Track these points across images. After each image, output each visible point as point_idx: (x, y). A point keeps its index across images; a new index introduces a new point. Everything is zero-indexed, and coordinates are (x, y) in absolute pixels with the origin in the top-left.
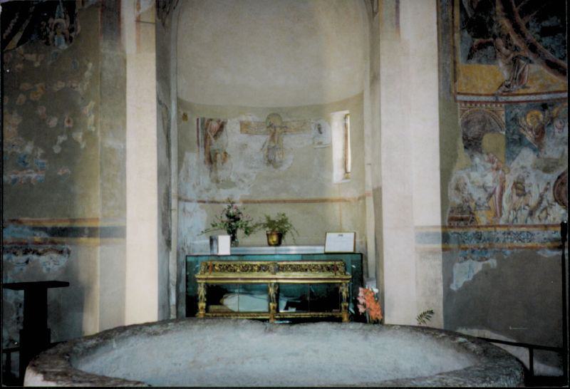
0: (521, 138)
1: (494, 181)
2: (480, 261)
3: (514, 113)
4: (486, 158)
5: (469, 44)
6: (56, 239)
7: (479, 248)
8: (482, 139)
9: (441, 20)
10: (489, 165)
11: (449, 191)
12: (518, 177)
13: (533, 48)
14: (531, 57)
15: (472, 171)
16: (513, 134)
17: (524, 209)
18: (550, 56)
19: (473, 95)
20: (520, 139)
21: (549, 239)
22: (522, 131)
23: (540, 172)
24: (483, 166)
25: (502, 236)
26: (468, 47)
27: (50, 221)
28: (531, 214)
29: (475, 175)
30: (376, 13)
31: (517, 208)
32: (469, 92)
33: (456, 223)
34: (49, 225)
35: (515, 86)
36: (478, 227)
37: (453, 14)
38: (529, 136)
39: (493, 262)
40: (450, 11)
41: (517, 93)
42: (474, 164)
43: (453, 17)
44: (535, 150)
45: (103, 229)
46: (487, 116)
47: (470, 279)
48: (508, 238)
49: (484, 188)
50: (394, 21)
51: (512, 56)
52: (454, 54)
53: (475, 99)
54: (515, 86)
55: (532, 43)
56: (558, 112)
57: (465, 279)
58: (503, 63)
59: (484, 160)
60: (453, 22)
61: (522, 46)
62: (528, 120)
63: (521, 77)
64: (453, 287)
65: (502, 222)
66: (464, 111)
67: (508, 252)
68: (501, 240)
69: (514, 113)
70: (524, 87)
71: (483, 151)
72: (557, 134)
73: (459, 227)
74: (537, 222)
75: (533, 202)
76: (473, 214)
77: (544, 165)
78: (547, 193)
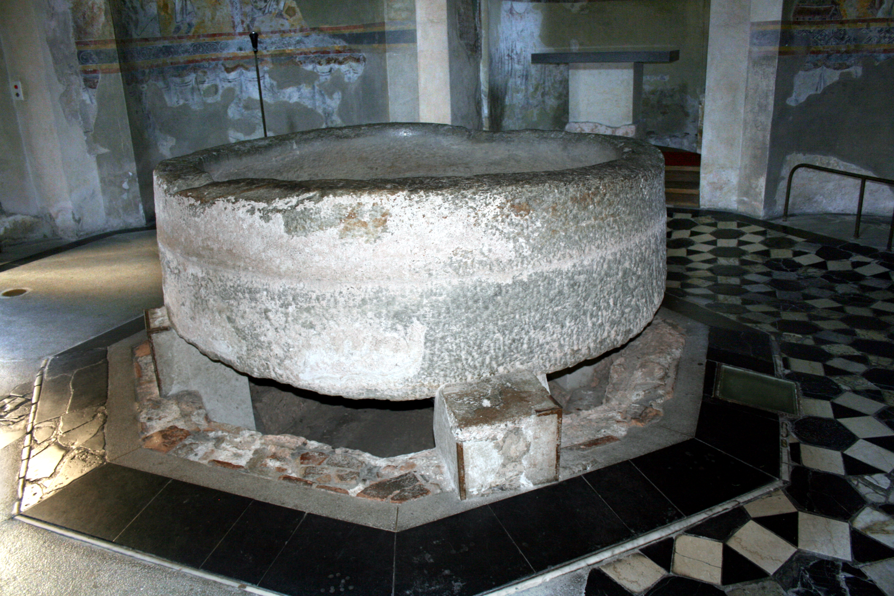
6: (354, 46)
7: (838, 52)
25: (878, 35)
27: (347, 28)
33: (807, 18)
34: (347, 32)
36: (842, 23)
39: (857, 71)
45: (392, 33)
47: (819, 92)
57: (812, 93)
67: (882, 57)
73: (811, 23)
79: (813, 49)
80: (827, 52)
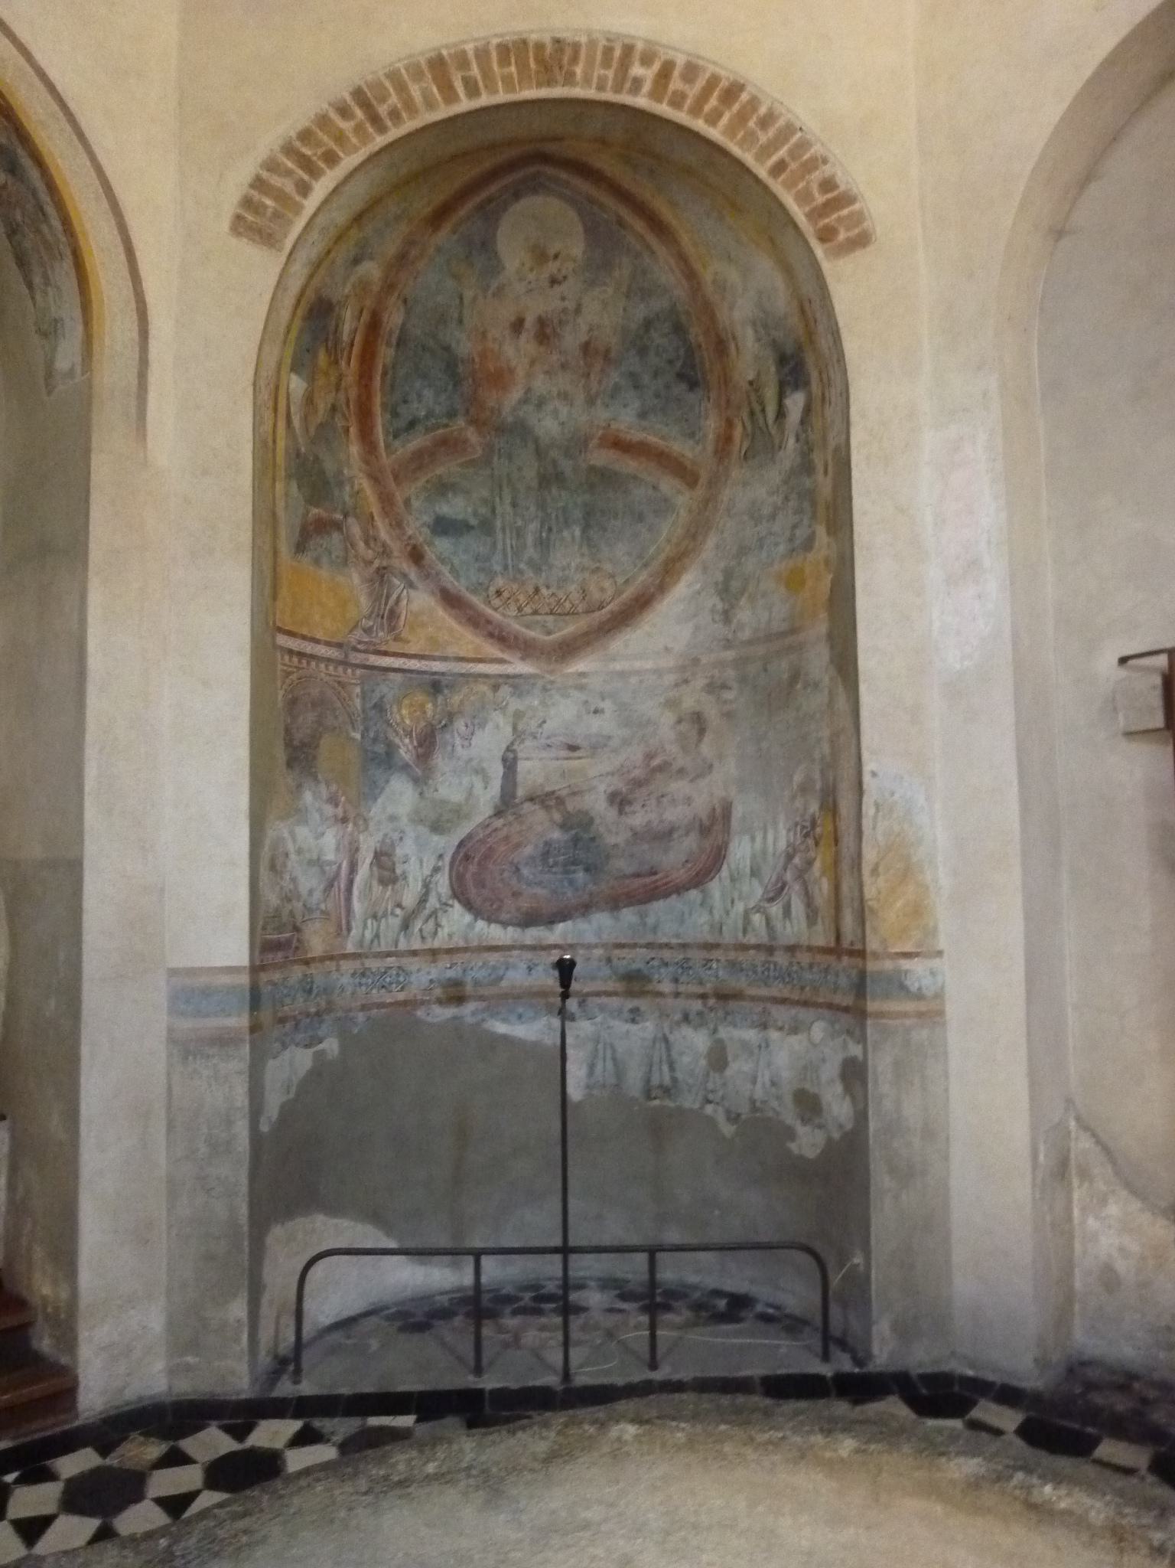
0: (391, 750)
1: (337, 849)
2: (306, 1046)
4: (323, 788)
8: (317, 747)
10: (329, 810)
12: (383, 842)
13: (416, 556)
16: (375, 740)
17: (393, 914)
18: (448, 579)
19: (304, 638)
21: (439, 981)
22: (392, 736)
23: (423, 830)
24: (320, 810)
25: (351, 980)
28: (406, 926)
29: (303, 832)
31: (380, 914)
36: (307, 962)
38: (406, 751)
39: (331, 1046)
43: (274, 441)
47: (292, 1096)
49: (318, 863)
50: (133, 411)
53: (308, 648)
56: (462, 701)
60: (274, 450)
61: (395, 546)
62: (404, 712)
64: (264, 1128)
65: (350, 948)
66: (288, 674)
67: (361, 1017)
68: (349, 990)
70: (397, 639)
71: (320, 777)
72: (459, 749)
73: (276, 966)
74: (417, 945)
75: (409, 899)
79: (280, 1014)
80: (294, 1017)
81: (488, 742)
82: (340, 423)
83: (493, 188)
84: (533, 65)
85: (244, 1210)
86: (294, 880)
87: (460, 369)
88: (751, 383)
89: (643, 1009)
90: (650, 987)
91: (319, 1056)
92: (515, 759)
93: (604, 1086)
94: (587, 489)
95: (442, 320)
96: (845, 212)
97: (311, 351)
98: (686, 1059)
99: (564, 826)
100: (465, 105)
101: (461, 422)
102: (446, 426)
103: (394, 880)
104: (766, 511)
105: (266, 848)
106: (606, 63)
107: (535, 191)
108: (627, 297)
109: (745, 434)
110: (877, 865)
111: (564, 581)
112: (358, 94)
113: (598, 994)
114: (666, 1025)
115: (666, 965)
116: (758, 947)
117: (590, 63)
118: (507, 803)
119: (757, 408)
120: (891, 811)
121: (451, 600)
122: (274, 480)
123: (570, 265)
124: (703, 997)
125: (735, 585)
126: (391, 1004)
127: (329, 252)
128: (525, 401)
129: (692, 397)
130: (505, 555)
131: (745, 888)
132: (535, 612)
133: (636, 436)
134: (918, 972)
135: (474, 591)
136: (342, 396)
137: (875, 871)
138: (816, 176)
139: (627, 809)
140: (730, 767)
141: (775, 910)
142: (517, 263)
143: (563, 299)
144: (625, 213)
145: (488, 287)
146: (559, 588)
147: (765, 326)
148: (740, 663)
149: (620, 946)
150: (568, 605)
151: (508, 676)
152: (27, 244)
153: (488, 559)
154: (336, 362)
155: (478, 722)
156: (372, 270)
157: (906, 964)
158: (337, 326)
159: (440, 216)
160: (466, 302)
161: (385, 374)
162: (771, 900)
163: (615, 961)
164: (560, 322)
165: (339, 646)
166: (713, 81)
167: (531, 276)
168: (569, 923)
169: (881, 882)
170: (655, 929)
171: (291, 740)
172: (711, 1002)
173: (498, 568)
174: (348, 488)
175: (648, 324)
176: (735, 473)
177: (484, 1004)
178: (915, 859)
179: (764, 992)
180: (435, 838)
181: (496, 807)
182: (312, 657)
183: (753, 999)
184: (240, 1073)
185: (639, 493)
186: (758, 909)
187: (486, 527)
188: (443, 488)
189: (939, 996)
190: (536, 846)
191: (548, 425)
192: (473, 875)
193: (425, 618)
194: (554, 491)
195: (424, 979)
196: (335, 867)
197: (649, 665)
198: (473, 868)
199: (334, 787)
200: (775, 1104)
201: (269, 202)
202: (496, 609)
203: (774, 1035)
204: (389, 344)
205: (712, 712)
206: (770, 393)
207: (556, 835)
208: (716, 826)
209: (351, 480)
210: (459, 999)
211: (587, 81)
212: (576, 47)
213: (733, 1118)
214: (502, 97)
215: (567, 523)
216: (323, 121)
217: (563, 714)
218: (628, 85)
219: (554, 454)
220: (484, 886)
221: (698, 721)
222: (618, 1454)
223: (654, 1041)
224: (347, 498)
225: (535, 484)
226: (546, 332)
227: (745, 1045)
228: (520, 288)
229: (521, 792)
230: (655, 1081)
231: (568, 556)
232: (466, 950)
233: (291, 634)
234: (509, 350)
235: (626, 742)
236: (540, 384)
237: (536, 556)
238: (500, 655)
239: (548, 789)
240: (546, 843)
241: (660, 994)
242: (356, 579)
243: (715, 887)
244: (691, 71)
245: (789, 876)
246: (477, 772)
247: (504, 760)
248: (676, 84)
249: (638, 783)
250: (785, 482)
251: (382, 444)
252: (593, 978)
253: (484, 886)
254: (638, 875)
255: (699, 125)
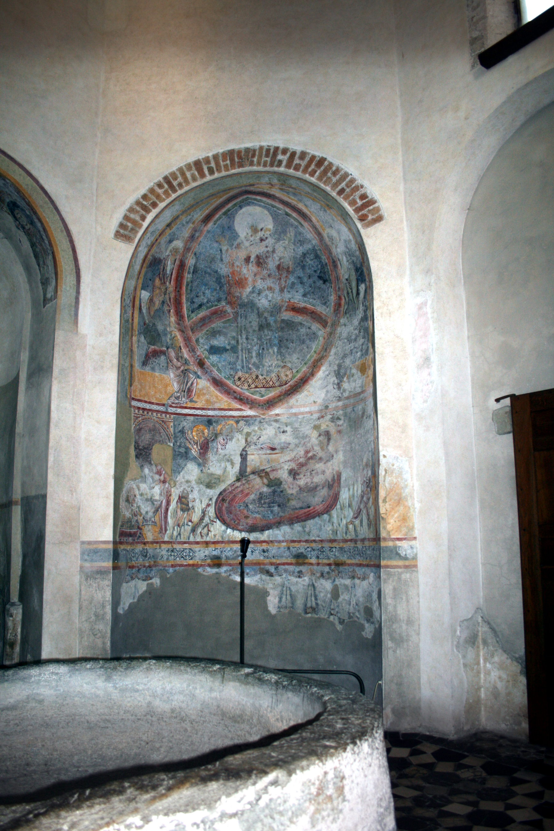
1: (161, 495)
2: (143, 580)
3: (181, 426)
5: (145, 349)
9: (123, 321)
10: (157, 477)
11: (121, 501)
13: (201, 364)
14: (199, 373)
15: (141, 482)
17: (187, 525)
19: (146, 402)
20: (186, 452)
23: (202, 487)
24: (152, 477)
26: (144, 352)
28: (193, 530)
29: (143, 486)
30: (51, 300)
32: (142, 398)
33: (125, 539)
35: (183, 399)
36: (145, 543)
37: (133, 316)
38: (195, 451)
39: (156, 581)
40: (131, 312)
41: (185, 405)
42: (143, 475)
43: (133, 320)
44: (199, 465)
46: (157, 425)
47: (136, 600)
48: (171, 555)
49: (151, 500)
50: (73, 313)
51: (182, 368)
52: (132, 357)
53: (148, 406)
54: (183, 399)
55: (200, 360)
57: (131, 601)
58: (174, 373)
59: (152, 471)
60: (132, 324)
61: (191, 361)
63: (190, 391)
64: (120, 611)
65: (166, 539)
66: (137, 418)
67: (171, 570)
68: (165, 557)
69: (181, 426)
70: (191, 401)
72: (220, 450)
73: (127, 543)
74: (199, 539)
75: (195, 518)
76: (141, 529)
77: (207, 480)
78: (209, 508)
79: (130, 564)
81: (234, 446)
82: (166, 308)
83: (230, 205)
84: (236, 160)
85: (109, 644)
86: (139, 507)
87: (223, 280)
88: (347, 280)
89: (303, 571)
90: (306, 561)
91: (150, 586)
92: (246, 454)
93: (286, 607)
94: (281, 330)
95: (213, 260)
96: (371, 207)
97: (152, 280)
98: (322, 595)
99: (268, 486)
100: (209, 178)
101: (224, 304)
102: (216, 305)
103: (188, 510)
104: (353, 337)
105: (124, 492)
106: (267, 155)
107: (248, 204)
108: (294, 244)
109: (346, 303)
110: (385, 498)
111: (269, 372)
112: (166, 178)
113: (284, 564)
114: (313, 578)
115: (314, 550)
116: (351, 540)
117: (260, 156)
118: (242, 475)
119: (350, 291)
120: (392, 472)
121: (217, 383)
122: (132, 336)
123: (268, 233)
124: (329, 565)
125: (342, 371)
126: (186, 565)
127: (157, 240)
128: (253, 292)
129: (323, 286)
130: (242, 361)
131: (346, 513)
132: (256, 387)
133: (303, 305)
134: (404, 547)
135: (228, 378)
136: (167, 296)
137: (384, 501)
138: (358, 194)
139: (297, 477)
140: (340, 457)
141: (357, 522)
142: (245, 234)
143: (267, 247)
144: (288, 210)
145: (233, 245)
146: (267, 375)
147: (349, 255)
148: (345, 407)
149: (293, 541)
150: (271, 383)
151: (244, 417)
152: (38, 250)
153: (235, 363)
154: (165, 283)
155: (229, 437)
156: (179, 244)
157: (398, 543)
158: (164, 268)
159: (207, 219)
160: (224, 252)
161: (187, 285)
162: (356, 518)
163: (291, 548)
164: (266, 257)
165: (164, 405)
166: (313, 157)
167: (252, 239)
168: (271, 531)
169: (387, 506)
170: (309, 534)
171: (138, 446)
172: (333, 567)
173: (239, 367)
174: (169, 336)
175: (304, 255)
176: (342, 321)
177: (231, 568)
178: (404, 495)
179: (353, 561)
180: (208, 490)
181: (237, 477)
182: (150, 410)
183: (349, 565)
184: (108, 586)
185: (303, 331)
186: (352, 523)
187: (234, 349)
188: (214, 333)
189: (415, 558)
190: (256, 495)
191: (263, 302)
192: (226, 508)
193: (205, 391)
194: (266, 331)
195: (202, 555)
196: (159, 503)
197: (307, 409)
198: (226, 505)
199: (159, 467)
200: (357, 614)
201: (129, 224)
202: (238, 386)
203: (357, 581)
204: (189, 273)
205: (333, 430)
206: (354, 284)
207: (265, 489)
208: (334, 483)
209: (171, 332)
210: (219, 565)
211: (259, 164)
212: (254, 151)
213: (341, 622)
214: (224, 173)
215: (272, 346)
216: (152, 191)
217: (268, 433)
218: (276, 163)
219: (266, 314)
220: (231, 513)
221: (327, 434)
222: (148, 669)
223: (309, 586)
224: (168, 340)
225: (257, 329)
226: (260, 261)
227: (346, 587)
228: (247, 244)
229: (249, 470)
230: (309, 605)
231: (271, 361)
232: (222, 542)
233: (139, 400)
234: (244, 271)
235: (297, 446)
236: (260, 284)
237: (257, 362)
238: (239, 407)
239: (262, 468)
240: (260, 493)
241: (311, 564)
242: (172, 375)
243: (334, 513)
244: (303, 155)
245: (362, 506)
246: (228, 461)
247: (241, 455)
248: (297, 161)
249: (302, 465)
250: (360, 323)
251: (186, 316)
252: (282, 557)
253: (231, 513)
254: (301, 508)
255: (307, 176)
